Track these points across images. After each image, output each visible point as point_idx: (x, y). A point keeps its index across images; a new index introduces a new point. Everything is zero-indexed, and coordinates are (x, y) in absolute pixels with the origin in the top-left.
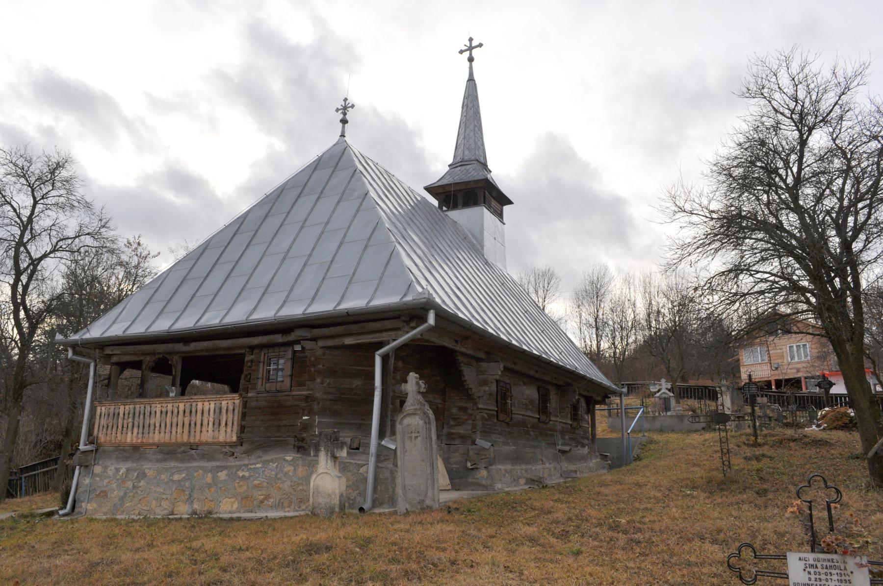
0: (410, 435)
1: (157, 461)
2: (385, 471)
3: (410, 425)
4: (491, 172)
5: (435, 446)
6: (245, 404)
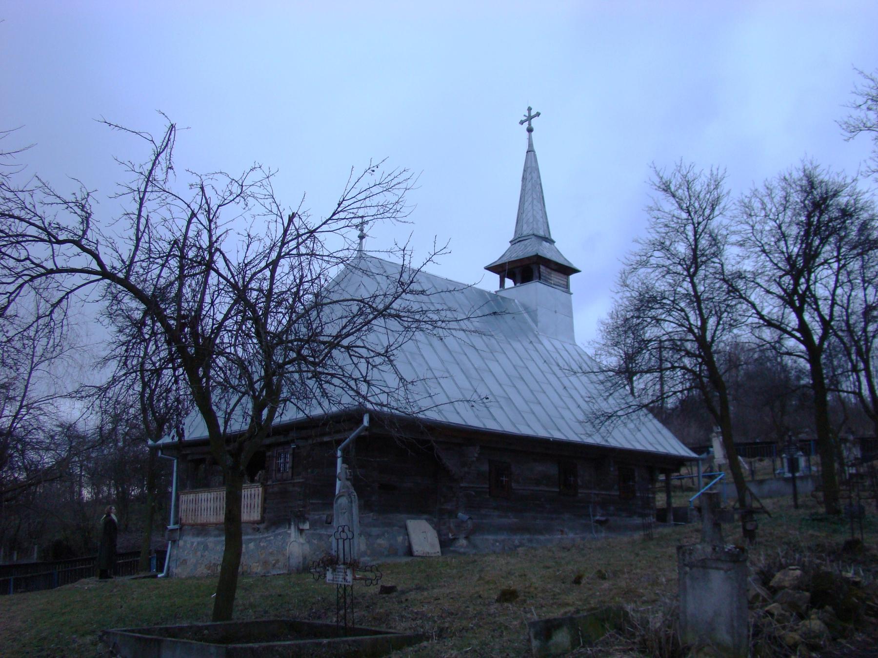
1: (216, 536)
4: (554, 242)
5: (356, 518)
6: (265, 491)
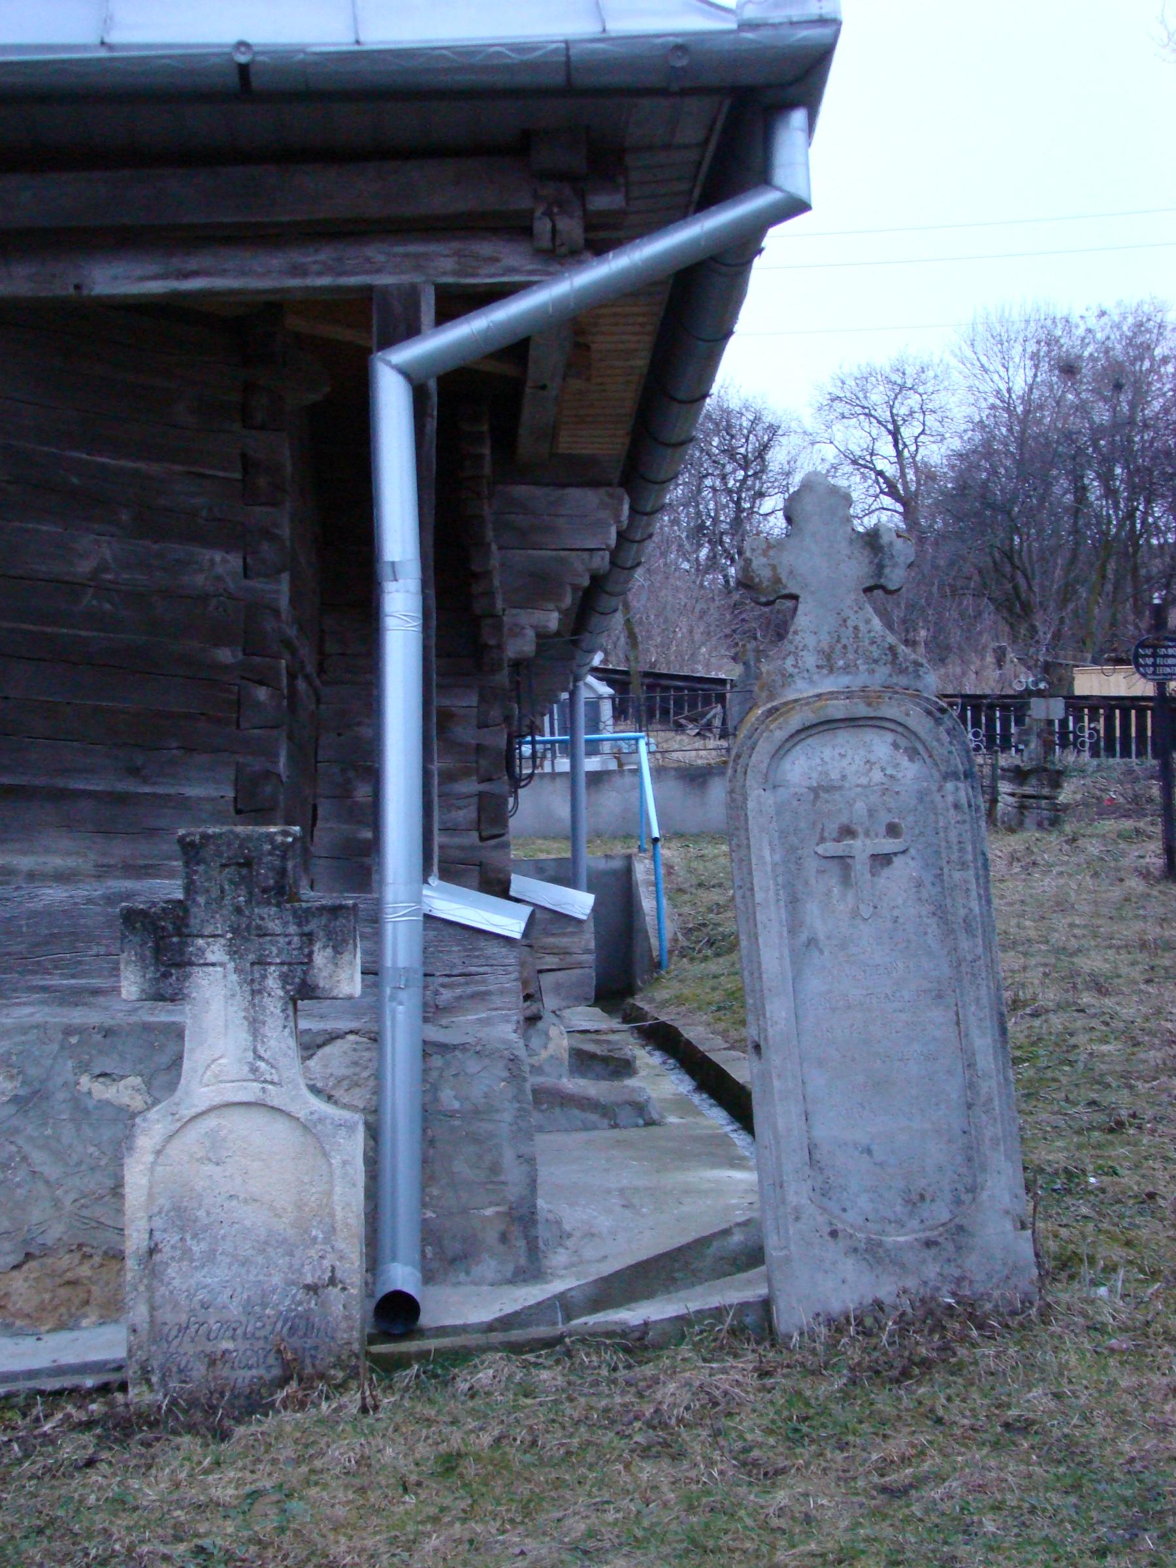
0: (830, 848)
2: (473, 1066)
3: (831, 789)
